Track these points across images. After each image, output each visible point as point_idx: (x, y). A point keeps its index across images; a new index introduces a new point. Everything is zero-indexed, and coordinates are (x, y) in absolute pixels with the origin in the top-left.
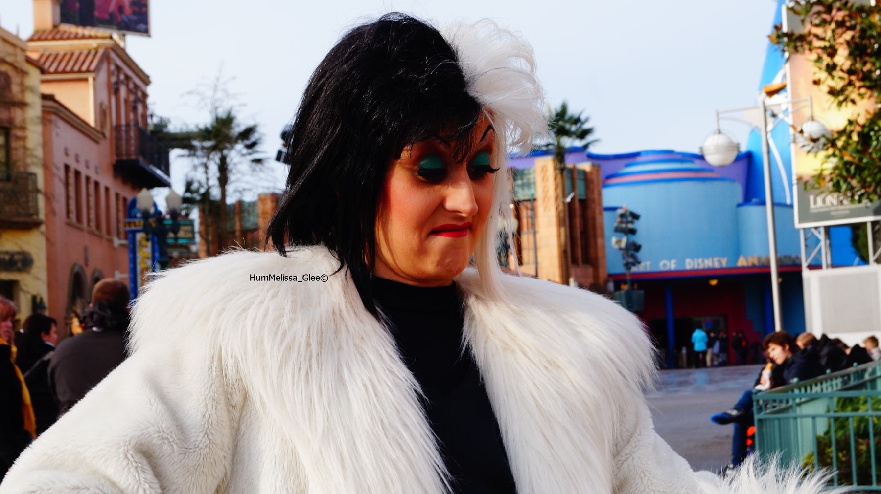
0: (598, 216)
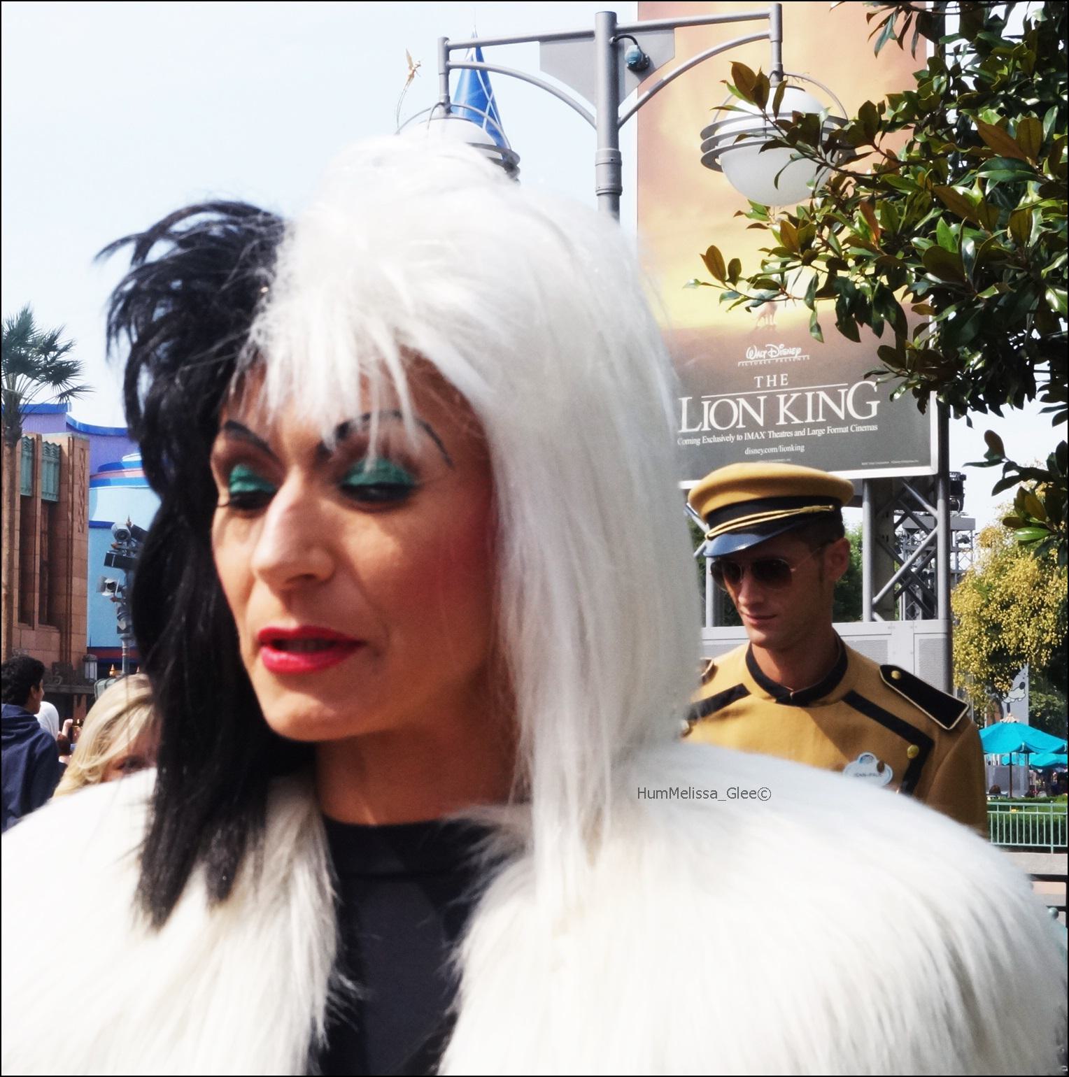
0: (76, 535)
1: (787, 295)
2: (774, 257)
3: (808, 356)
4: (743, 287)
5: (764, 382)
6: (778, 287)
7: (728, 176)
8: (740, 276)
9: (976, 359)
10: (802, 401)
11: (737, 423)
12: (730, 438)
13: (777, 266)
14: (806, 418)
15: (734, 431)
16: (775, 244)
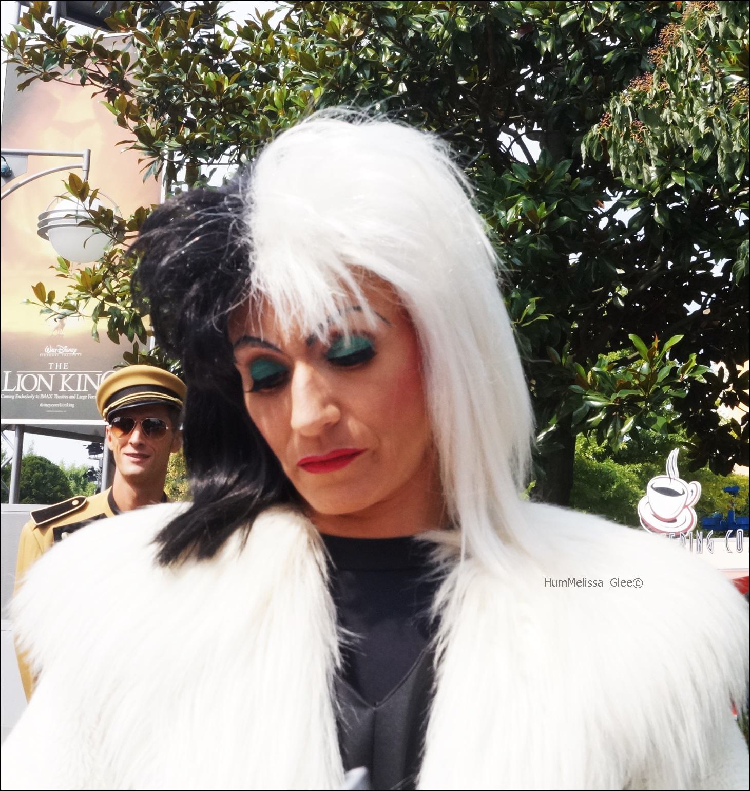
1: (79, 313)
2: (77, 291)
3: (81, 354)
4: (54, 307)
5: (54, 366)
6: (74, 309)
7: (52, 243)
8: (54, 300)
9: (176, 364)
10: (76, 378)
11: (37, 388)
12: (32, 397)
13: (75, 296)
14: (76, 389)
15: (35, 393)
16: (76, 283)
